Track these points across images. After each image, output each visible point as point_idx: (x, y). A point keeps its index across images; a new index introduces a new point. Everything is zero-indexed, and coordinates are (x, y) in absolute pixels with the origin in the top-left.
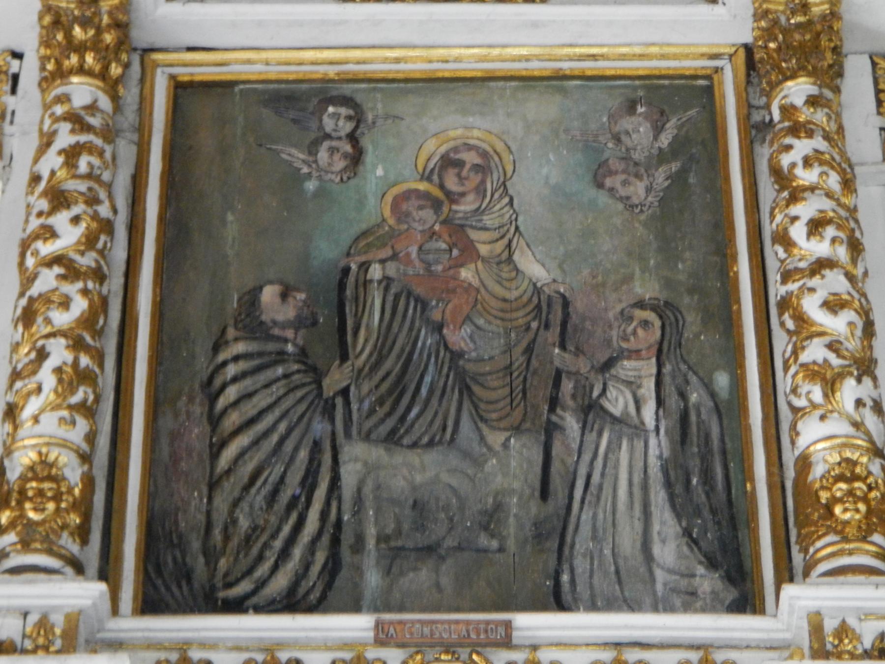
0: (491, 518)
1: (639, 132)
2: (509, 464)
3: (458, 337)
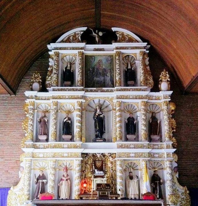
0: (101, 82)
2: (102, 78)
3: (100, 71)
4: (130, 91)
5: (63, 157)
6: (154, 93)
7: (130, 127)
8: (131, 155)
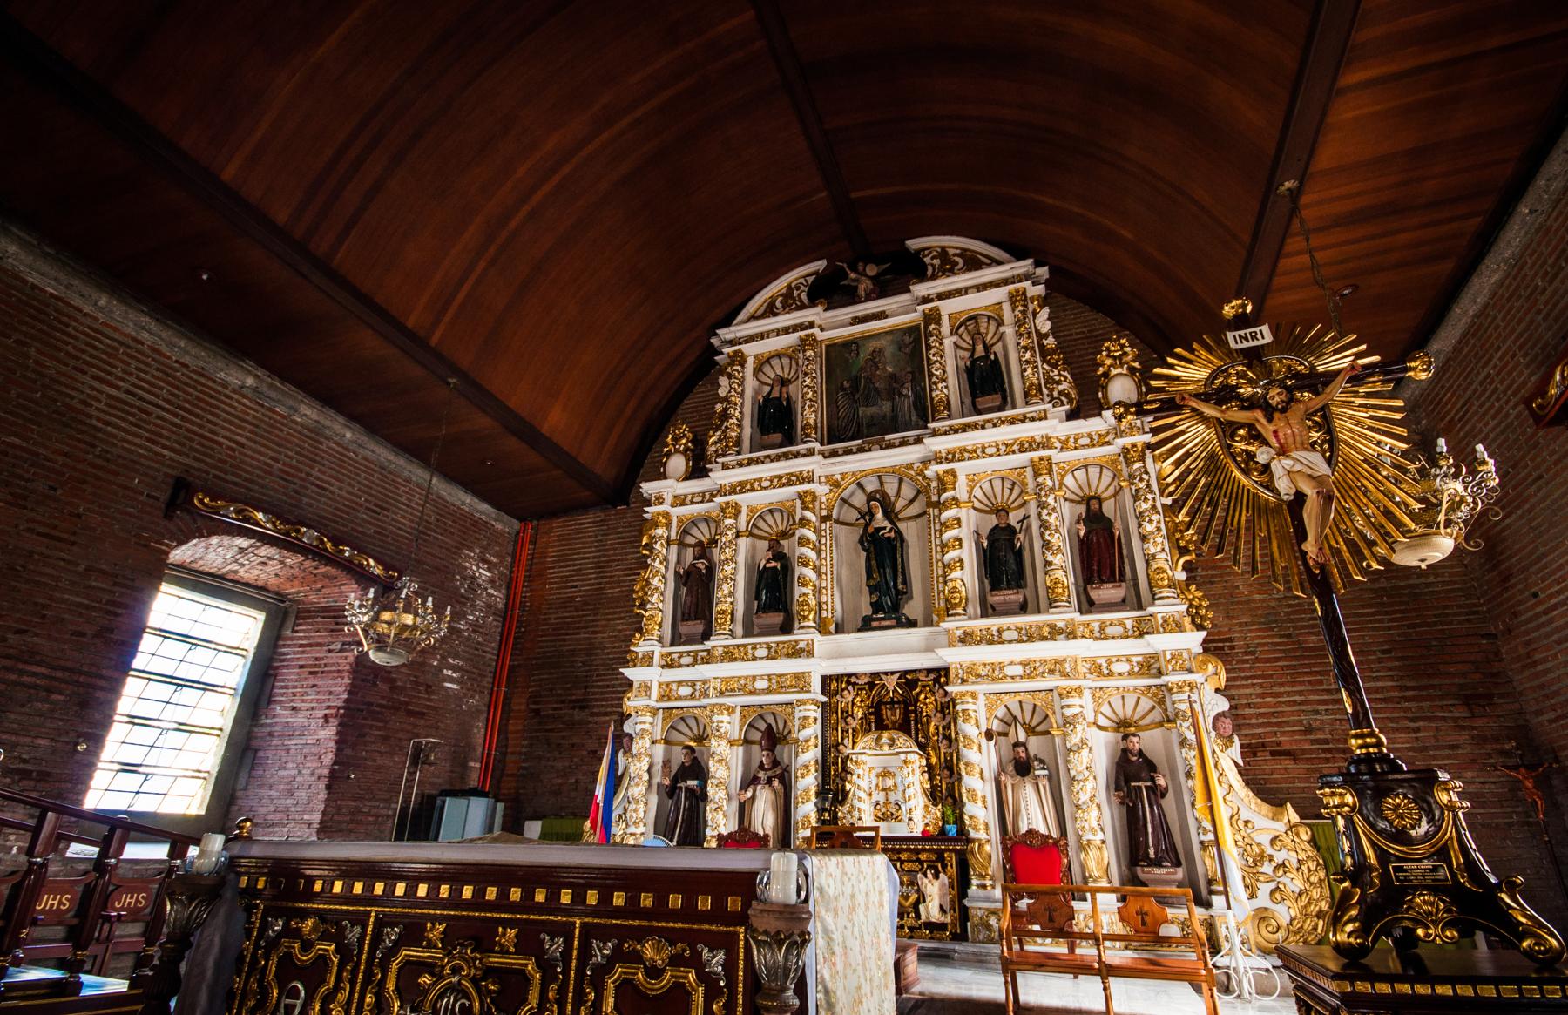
0: (884, 417)
1: (907, 338)
2: (886, 407)
4: (983, 427)
5: (753, 693)
6: (1081, 422)
7: (1004, 562)
8: (1009, 671)
